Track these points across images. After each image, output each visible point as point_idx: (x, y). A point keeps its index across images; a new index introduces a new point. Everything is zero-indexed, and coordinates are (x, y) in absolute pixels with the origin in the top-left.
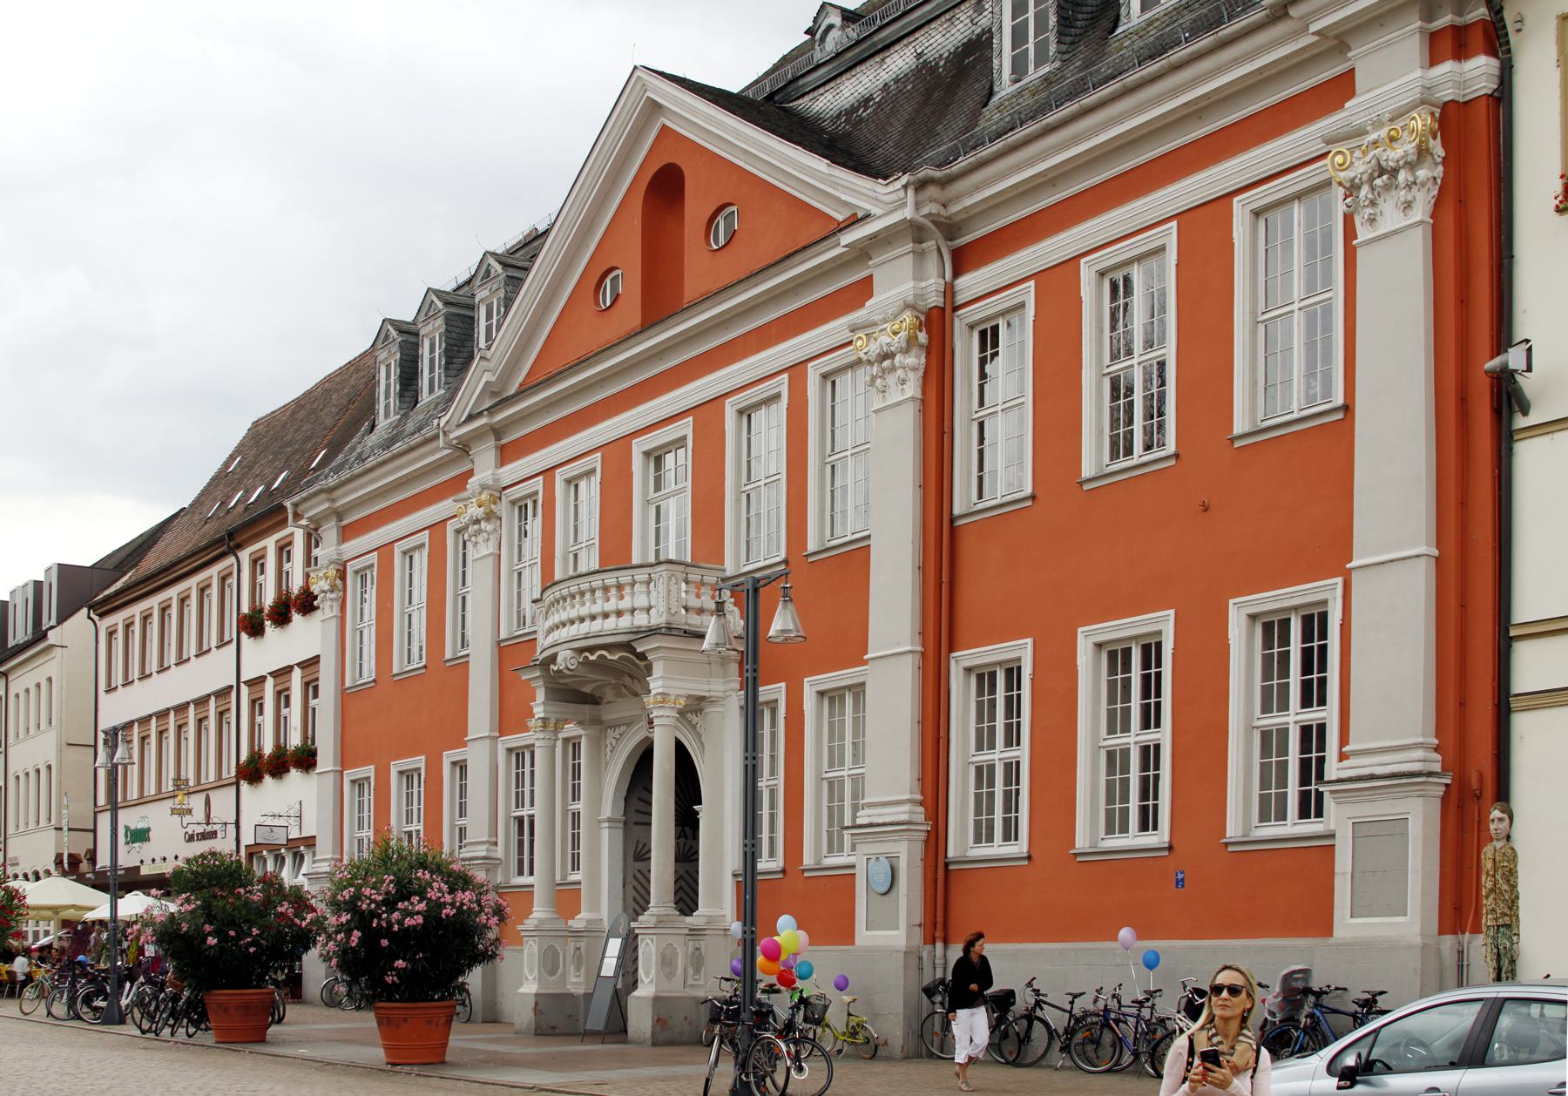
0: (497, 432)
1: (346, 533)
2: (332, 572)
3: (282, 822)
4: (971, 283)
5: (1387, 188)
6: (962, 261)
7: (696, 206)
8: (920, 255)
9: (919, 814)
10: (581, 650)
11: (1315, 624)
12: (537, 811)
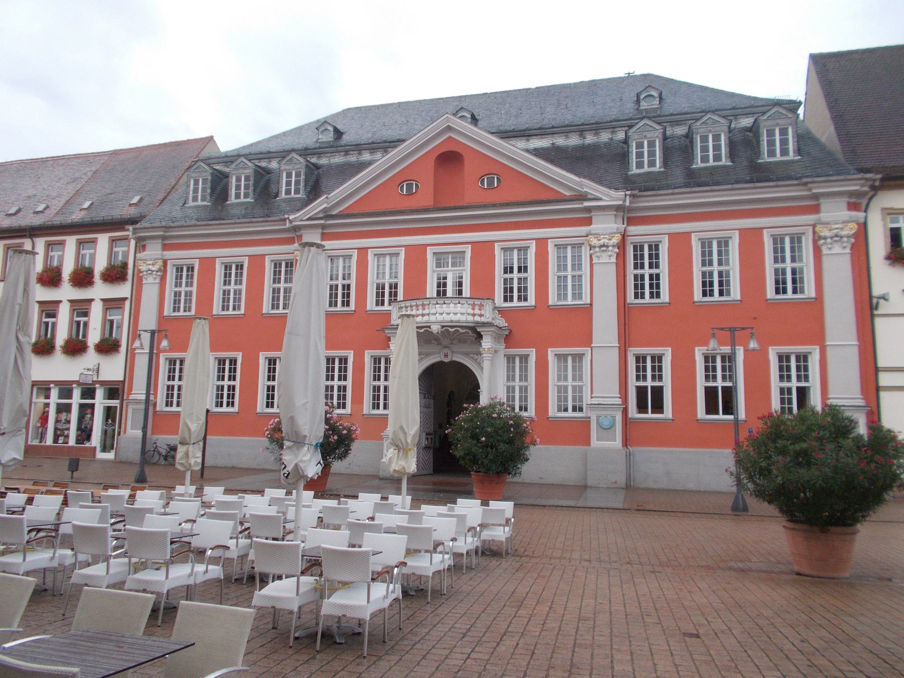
0: (323, 227)
1: (165, 247)
2: (160, 263)
3: (90, 373)
4: (633, 230)
5: (836, 241)
6: (631, 221)
7: (470, 168)
8: (615, 215)
9: (619, 401)
10: (443, 327)
11: (803, 359)
12: (349, 383)
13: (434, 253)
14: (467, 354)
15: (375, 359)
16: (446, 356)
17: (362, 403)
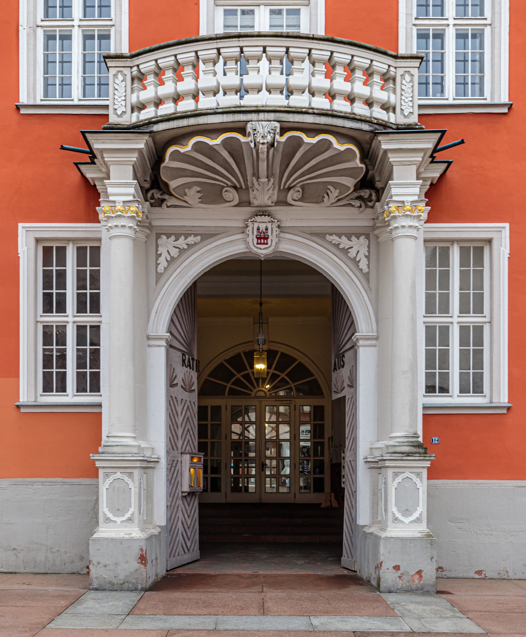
14: (319, 235)
15: (47, 251)
16: (262, 238)
17: (14, 372)
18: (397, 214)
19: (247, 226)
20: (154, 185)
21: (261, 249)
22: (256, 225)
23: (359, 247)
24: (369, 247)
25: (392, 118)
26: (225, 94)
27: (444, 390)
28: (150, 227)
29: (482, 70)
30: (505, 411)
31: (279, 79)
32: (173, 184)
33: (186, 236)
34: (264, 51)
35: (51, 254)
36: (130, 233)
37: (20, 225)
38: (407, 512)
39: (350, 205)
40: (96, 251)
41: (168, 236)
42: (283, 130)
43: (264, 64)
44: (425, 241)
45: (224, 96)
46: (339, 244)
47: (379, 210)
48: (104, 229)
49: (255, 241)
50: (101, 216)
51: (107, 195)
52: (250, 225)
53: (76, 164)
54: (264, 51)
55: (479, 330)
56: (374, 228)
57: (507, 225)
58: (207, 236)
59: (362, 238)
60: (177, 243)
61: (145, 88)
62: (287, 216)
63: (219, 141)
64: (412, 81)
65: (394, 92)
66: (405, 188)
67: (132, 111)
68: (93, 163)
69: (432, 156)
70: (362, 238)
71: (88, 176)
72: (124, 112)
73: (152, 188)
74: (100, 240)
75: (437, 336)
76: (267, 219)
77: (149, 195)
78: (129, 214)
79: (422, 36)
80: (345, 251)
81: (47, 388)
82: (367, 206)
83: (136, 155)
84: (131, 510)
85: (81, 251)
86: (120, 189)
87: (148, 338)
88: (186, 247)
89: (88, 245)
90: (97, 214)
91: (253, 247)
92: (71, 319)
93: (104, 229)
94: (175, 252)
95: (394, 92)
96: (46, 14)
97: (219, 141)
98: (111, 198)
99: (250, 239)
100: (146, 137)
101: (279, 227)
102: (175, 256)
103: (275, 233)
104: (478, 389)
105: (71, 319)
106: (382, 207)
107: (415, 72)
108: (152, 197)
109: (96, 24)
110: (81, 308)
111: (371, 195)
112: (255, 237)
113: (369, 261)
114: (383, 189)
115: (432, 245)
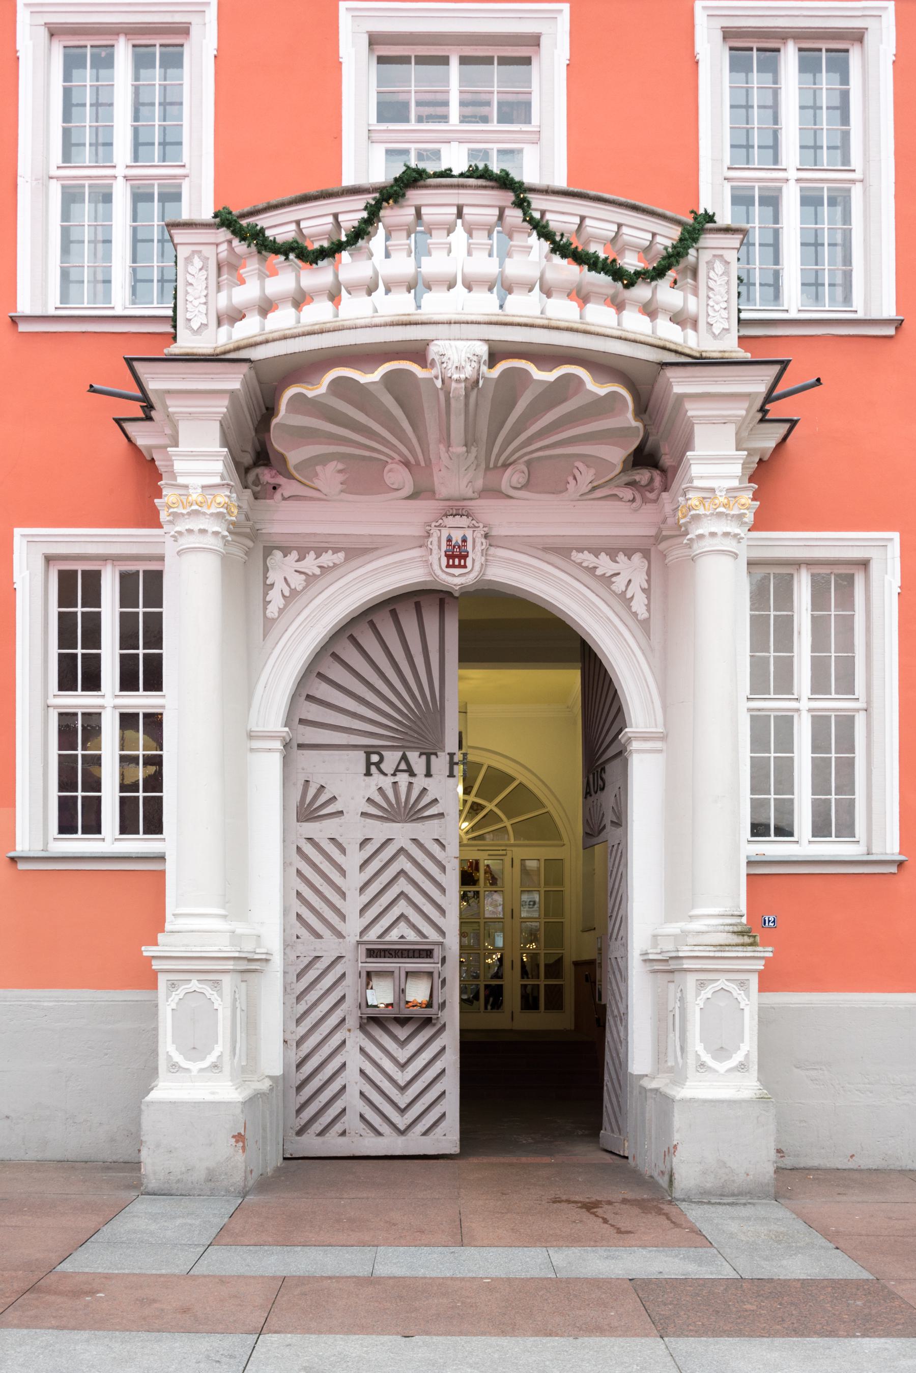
13: (374, 40)
14: (559, 550)
15: (66, 580)
16: (457, 555)
18: (701, 511)
19: (429, 535)
20: (256, 457)
21: (454, 575)
22: (445, 533)
23: (631, 572)
24: (648, 573)
25: (692, 341)
26: (388, 291)
27: (784, 831)
28: (254, 535)
29: (847, 260)
30: (894, 869)
31: (487, 266)
32: (294, 457)
33: (319, 552)
34: (460, 215)
35: (76, 586)
36: (215, 544)
37: (18, 532)
38: (721, 1053)
39: (614, 496)
40: (155, 580)
41: (286, 551)
42: (494, 358)
43: (459, 235)
44: (751, 563)
45: (386, 294)
46: (596, 568)
47: (668, 509)
48: (168, 540)
49: (444, 560)
50: (164, 516)
51: (173, 476)
52: (435, 533)
53: (118, 421)
54: (460, 215)
55: (847, 723)
56: (659, 538)
57: (896, 536)
58: (357, 551)
59: (637, 557)
60: (301, 566)
61: (242, 282)
62: (503, 518)
63: (376, 375)
64: (726, 273)
65: (696, 293)
66: (715, 463)
67: (219, 324)
68: (149, 418)
69: (762, 410)
70: (637, 557)
71: (140, 442)
72: (204, 326)
73: (256, 464)
74: (161, 558)
75: (770, 733)
76: (464, 522)
77: (251, 477)
78: (214, 510)
79: (741, 199)
80: (607, 580)
81: (66, 827)
82: (645, 501)
83: (226, 402)
84: (218, 1049)
85: (127, 581)
86: (198, 463)
87: (251, 736)
88: (318, 571)
89: (141, 567)
90: (157, 513)
91: (439, 572)
92: (110, 700)
93: (168, 540)
94: (297, 582)
95: (696, 293)
96: (67, 156)
97: (376, 375)
98: (181, 480)
99: (434, 559)
100: (245, 367)
101: (486, 536)
102: (299, 588)
103: (479, 548)
104: (847, 829)
105: (110, 700)
106: (674, 500)
107: (732, 256)
108: (257, 482)
109: (155, 170)
110: (128, 682)
111: (652, 480)
112: (443, 554)
113: (648, 598)
114: (676, 469)
115: (760, 572)
